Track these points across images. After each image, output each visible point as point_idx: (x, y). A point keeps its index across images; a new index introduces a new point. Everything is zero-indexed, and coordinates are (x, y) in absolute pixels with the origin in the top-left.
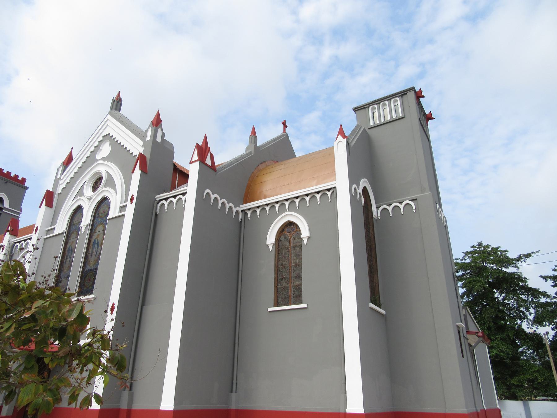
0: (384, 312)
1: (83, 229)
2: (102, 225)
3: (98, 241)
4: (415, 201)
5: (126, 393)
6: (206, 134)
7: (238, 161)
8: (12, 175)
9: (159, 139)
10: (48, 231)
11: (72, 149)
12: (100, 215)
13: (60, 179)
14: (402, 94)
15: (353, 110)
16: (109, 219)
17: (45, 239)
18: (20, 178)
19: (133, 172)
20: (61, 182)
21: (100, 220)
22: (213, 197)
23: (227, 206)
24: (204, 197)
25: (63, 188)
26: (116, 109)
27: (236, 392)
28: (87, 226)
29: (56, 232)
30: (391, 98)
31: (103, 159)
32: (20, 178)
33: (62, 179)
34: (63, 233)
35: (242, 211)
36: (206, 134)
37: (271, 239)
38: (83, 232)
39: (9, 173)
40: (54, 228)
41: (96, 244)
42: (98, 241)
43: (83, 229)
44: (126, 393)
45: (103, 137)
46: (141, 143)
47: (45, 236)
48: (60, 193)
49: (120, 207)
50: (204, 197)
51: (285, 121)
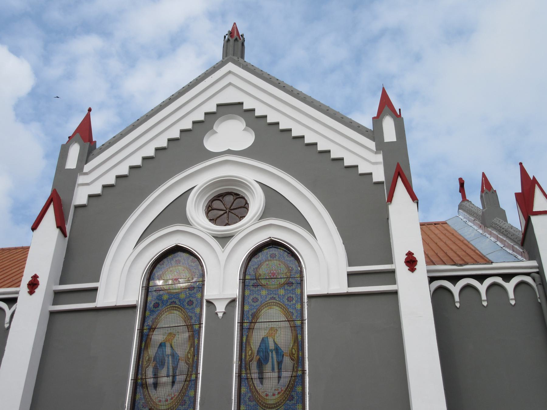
1: (221, 308)
2: (276, 308)
3: (275, 343)
6: (521, 164)
10: (57, 293)
11: (90, 110)
12: (263, 282)
13: (79, 169)
16: (310, 297)
17: (52, 313)
19: (390, 199)
20: (81, 179)
21: (264, 292)
25: (90, 196)
28: (233, 301)
29: (102, 301)
31: (229, 152)
33: (86, 174)
34: (134, 307)
36: (521, 164)
38: (220, 315)
40: (95, 290)
41: (272, 351)
42: (275, 343)
43: (221, 308)
45: (218, 106)
46: (372, 145)
47: (51, 305)
48: (83, 206)
49: (348, 272)
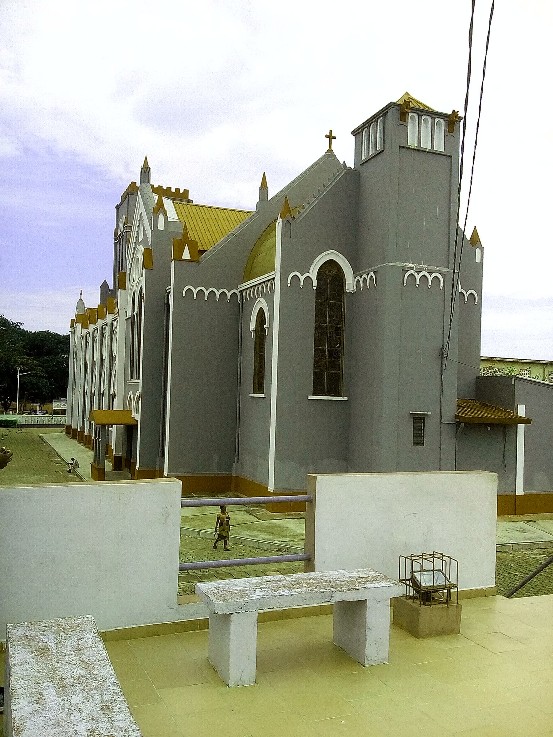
0: (346, 399)
4: (376, 274)
5: (158, 459)
7: (234, 235)
8: (173, 190)
9: (161, 227)
14: (383, 113)
15: (352, 134)
18: (181, 191)
22: (195, 292)
23: (218, 294)
24: (184, 295)
26: (145, 182)
27: (238, 462)
30: (378, 119)
32: (181, 191)
34: (130, 317)
35: (240, 291)
37: (253, 326)
39: (169, 189)
44: (158, 459)
50: (184, 295)
51: (331, 131)
